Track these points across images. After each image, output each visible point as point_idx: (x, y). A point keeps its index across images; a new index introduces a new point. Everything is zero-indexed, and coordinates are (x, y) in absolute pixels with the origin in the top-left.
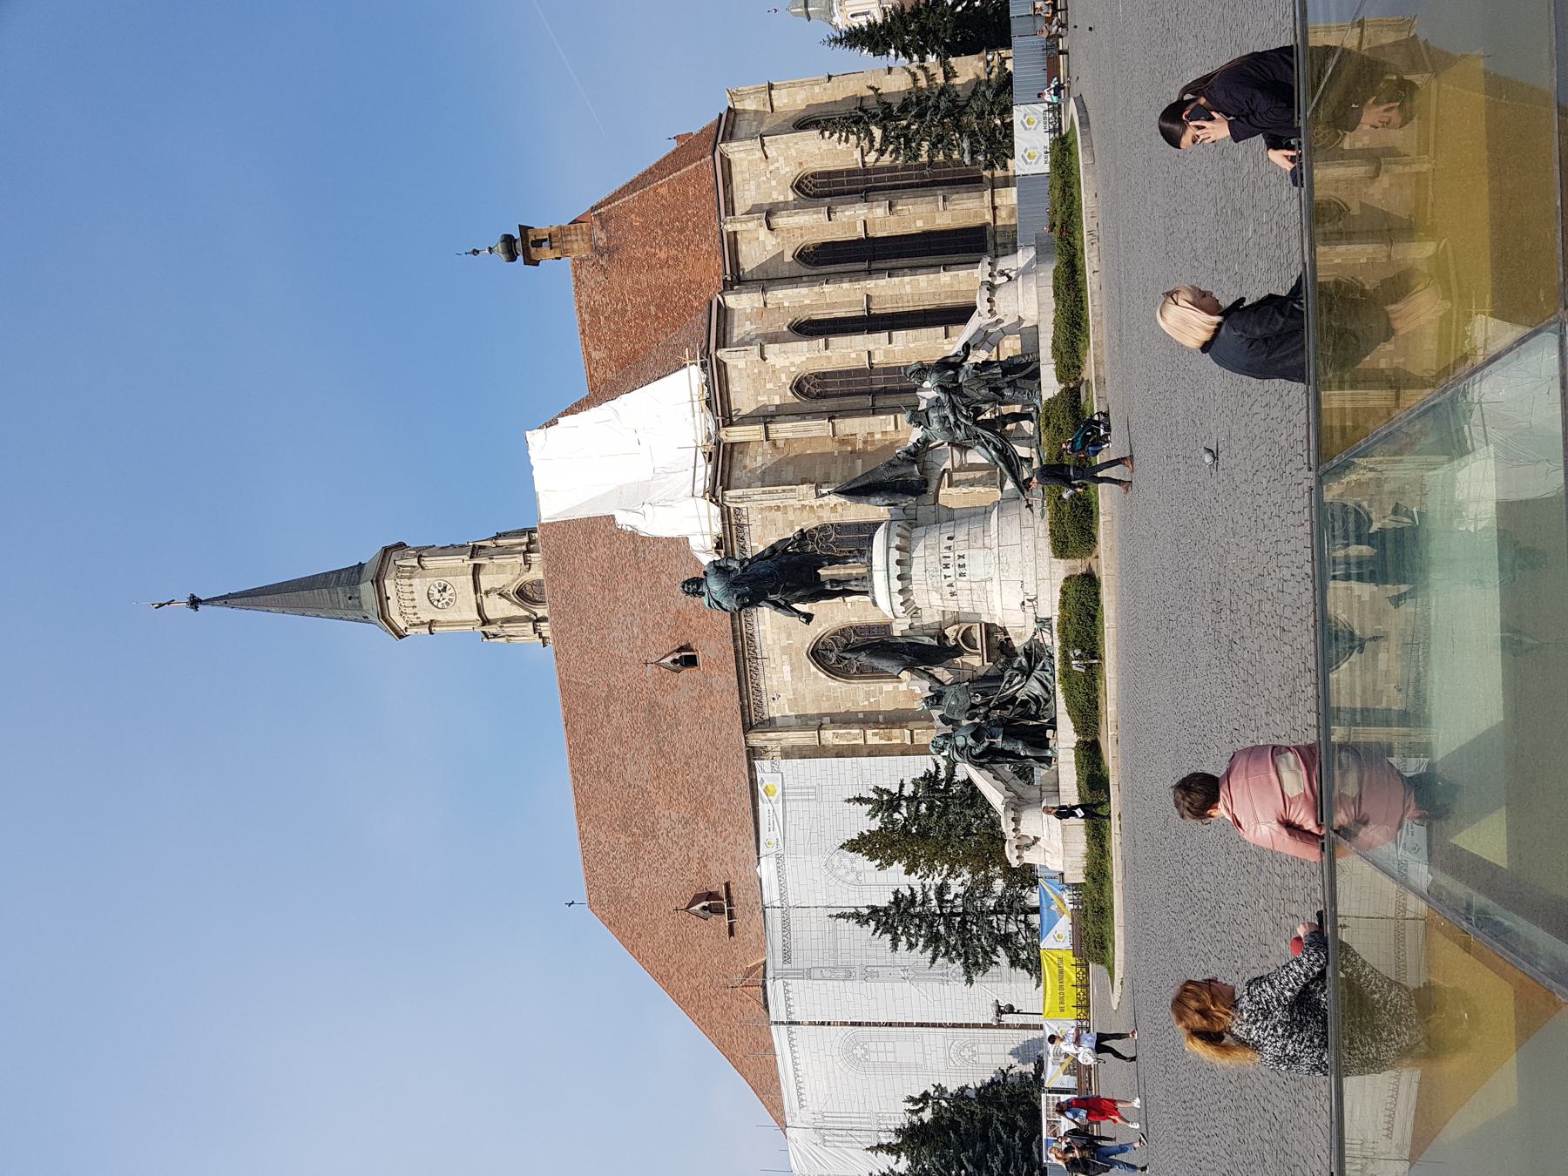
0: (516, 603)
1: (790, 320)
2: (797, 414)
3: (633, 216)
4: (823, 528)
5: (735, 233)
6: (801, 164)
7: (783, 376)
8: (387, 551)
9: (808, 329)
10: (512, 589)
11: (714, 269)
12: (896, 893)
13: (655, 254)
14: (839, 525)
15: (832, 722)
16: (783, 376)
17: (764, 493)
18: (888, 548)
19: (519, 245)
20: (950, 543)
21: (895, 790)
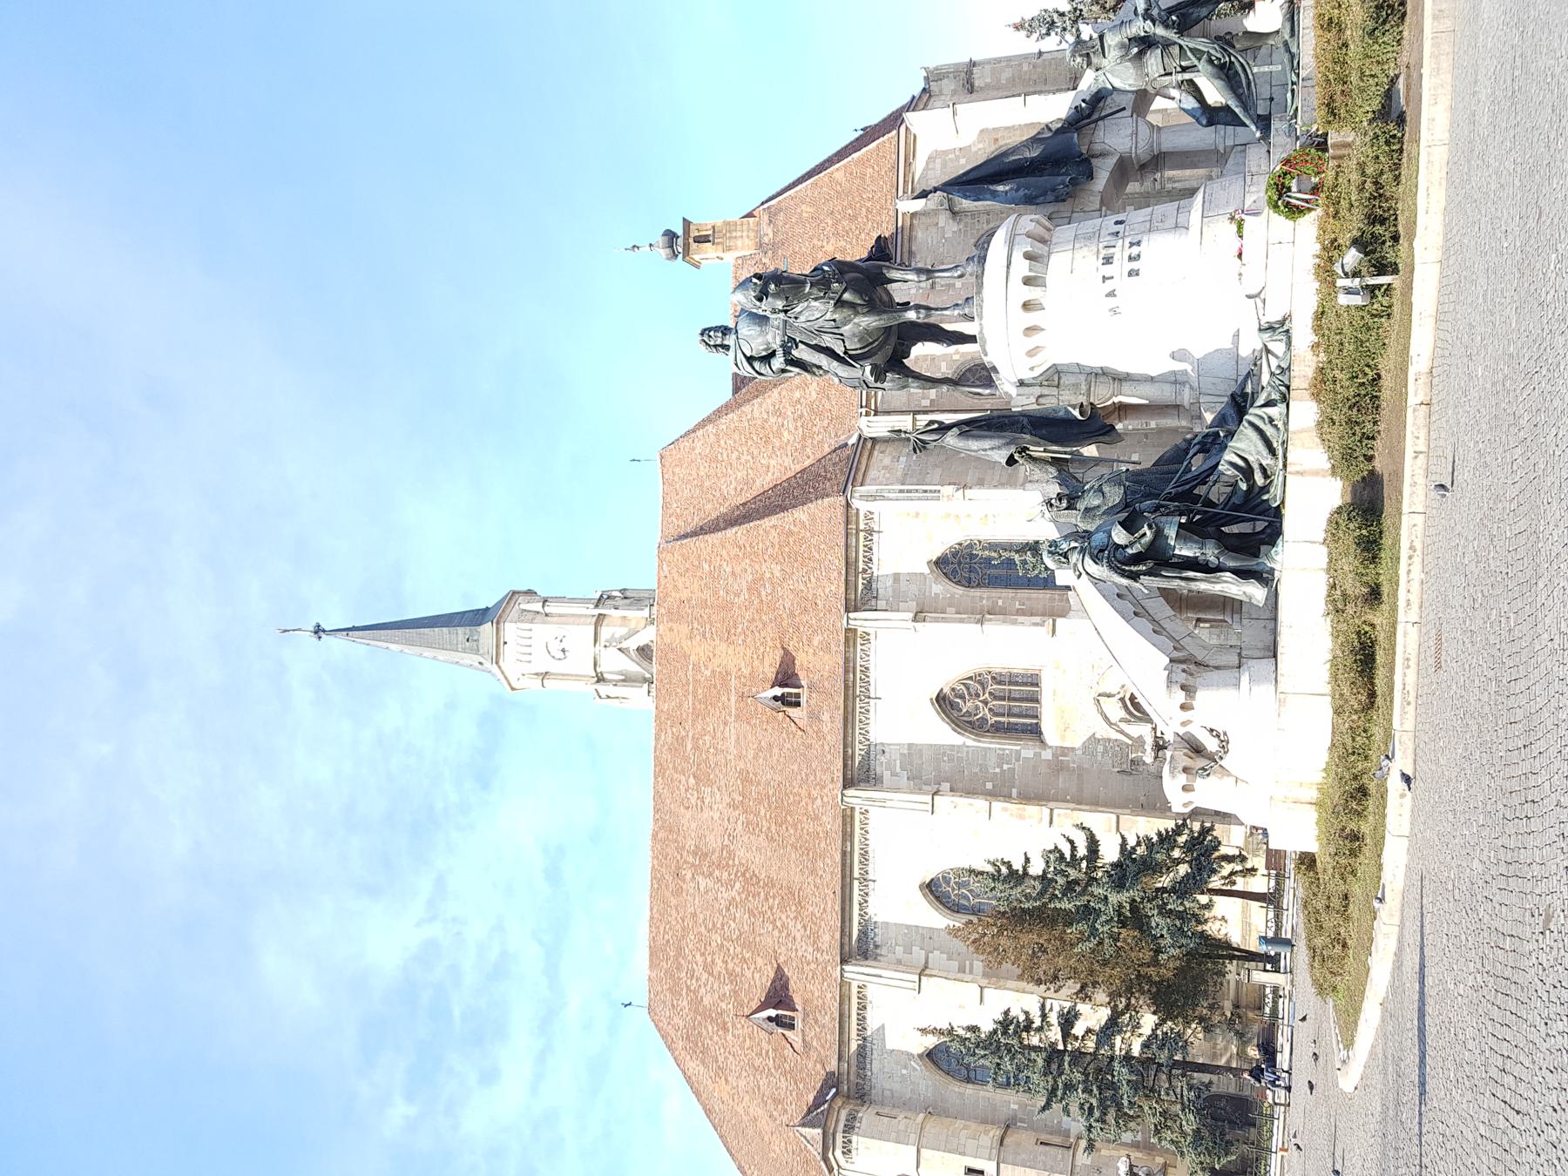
0: (633, 660)
3: (804, 207)
6: (996, 140)
7: (943, 365)
8: (514, 593)
10: (633, 644)
12: (1007, 1013)
16: (943, 365)
17: (901, 491)
19: (680, 241)
21: (1018, 865)
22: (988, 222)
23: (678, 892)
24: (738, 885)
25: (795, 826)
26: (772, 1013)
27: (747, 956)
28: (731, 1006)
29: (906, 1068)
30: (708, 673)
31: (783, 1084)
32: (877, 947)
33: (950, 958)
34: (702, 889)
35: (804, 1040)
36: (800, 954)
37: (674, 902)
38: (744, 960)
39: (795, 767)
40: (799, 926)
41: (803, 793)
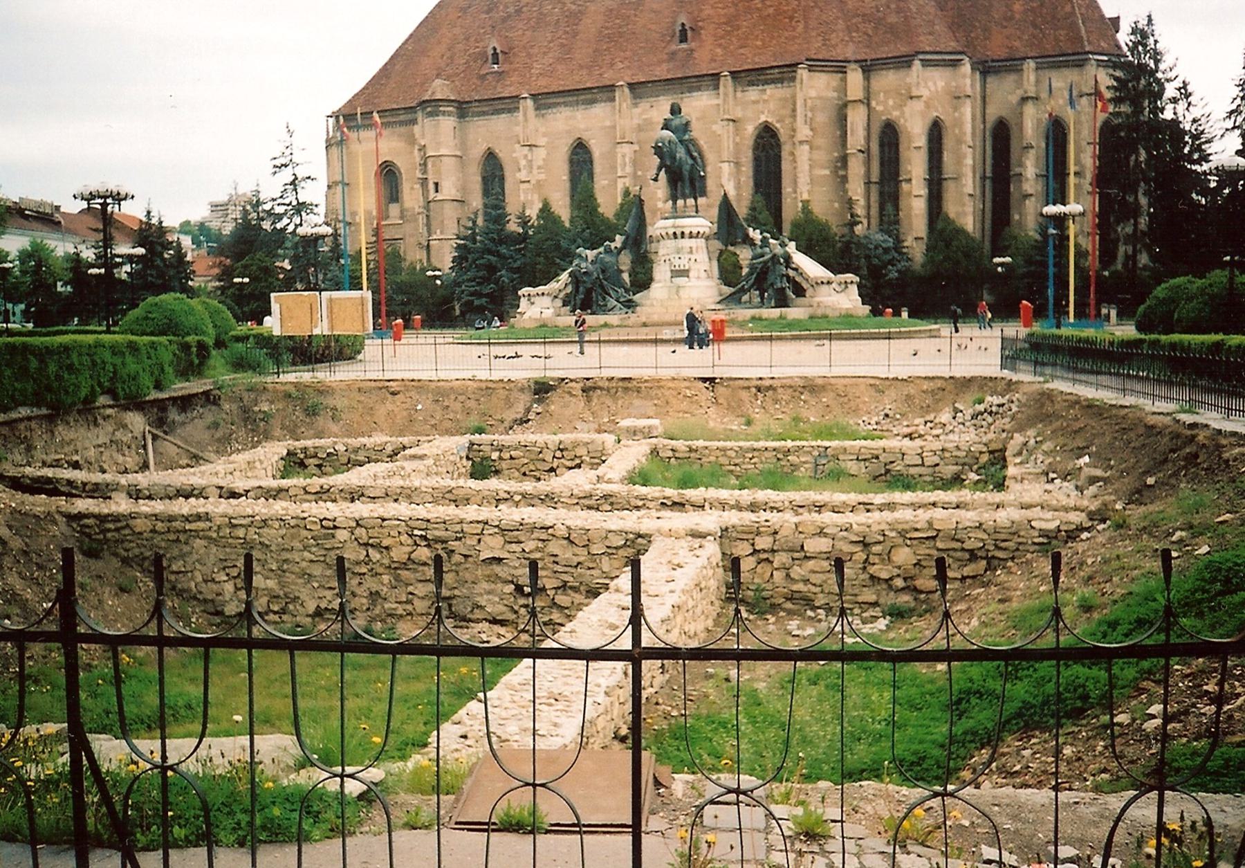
1: (942, 117)
2: (868, 125)
5: (1022, 70)
9: (936, 133)
11: (996, 48)
14: (780, 157)
15: (635, 151)
17: (805, 100)
18: (690, 226)
20: (693, 260)
22: (1016, 124)
24: (574, 7)
26: (498, 51)
32: (543, 115)
33: (544, 160)
38: (530, 19)
40: (551, 61)
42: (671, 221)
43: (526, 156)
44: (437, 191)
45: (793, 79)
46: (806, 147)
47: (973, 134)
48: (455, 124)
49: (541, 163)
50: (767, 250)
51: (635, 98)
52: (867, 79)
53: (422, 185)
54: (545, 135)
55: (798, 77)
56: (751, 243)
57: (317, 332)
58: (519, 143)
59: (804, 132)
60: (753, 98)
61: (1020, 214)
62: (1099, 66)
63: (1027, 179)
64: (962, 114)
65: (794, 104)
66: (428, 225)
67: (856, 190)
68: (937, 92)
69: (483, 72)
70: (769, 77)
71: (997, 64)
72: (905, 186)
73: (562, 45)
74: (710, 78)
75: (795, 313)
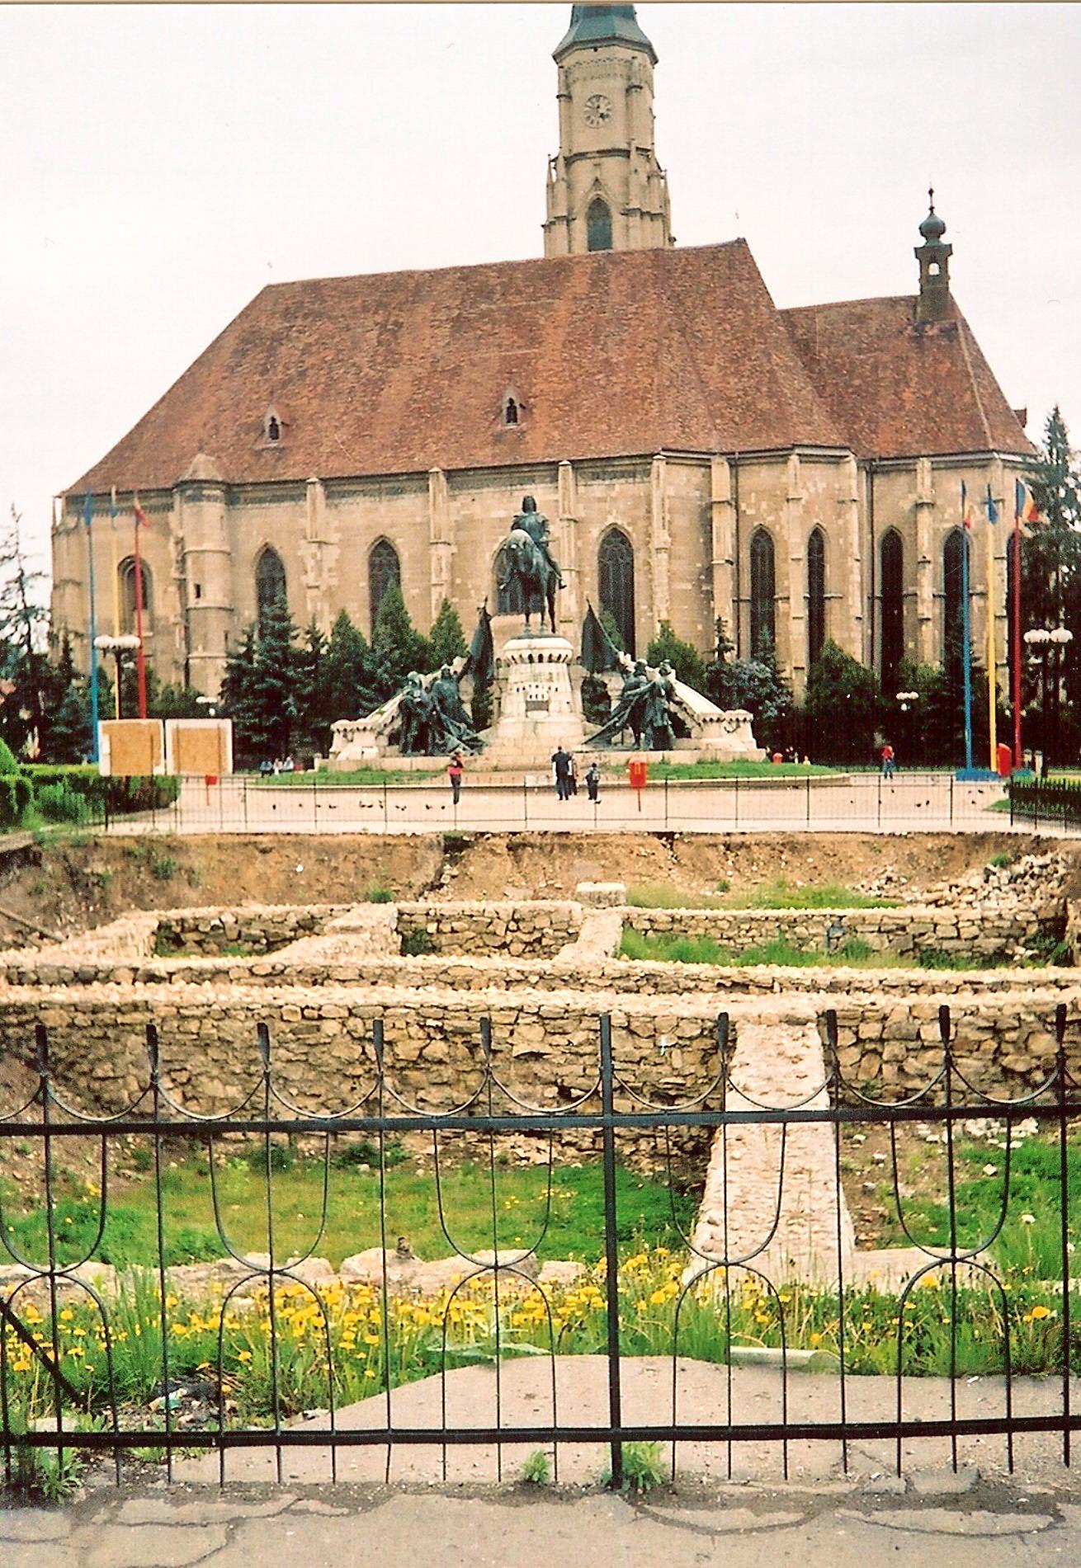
1: (824, 525)
3: (949, 365)
4: (631, 553)
11: (884, 444)
13: (909, 387)
16: (771, 518)
17: (663, 500)
23: (365, 309)
24: (372, 373)
25: (416, 427)
26: (278, 422)
27: (319, 389)
28: (280, 376)
29: (258, 534)
30: (542, 322)
31: (230, 433)
32: (336, 506)
34: (368, 335)
35: (263, 450)
36: (324, 440)
37: (358, 303)
39: (461, 423)
41: (444, 433)
42: (525, 642)
43: (314, 556)
44: (198, 596)
45: (648, 473)
46: (664, 556)
47: (861, 546)
48: (222, 512)
49: (333, 565)
50: (643, 678)
51: (452, 488)
52: (735, 476)
53: (180, 588)
54: (337, 530)
55: (654, 470)
56: (624, 671)
57: (159, 771)
58: (305, 538)
59: (661, 537)
60: (599, 495)
61: (916, 642)
62: (1005, 467)
63: (923, 601)
64: (846, 522)
65: (649, 504)
66: (187, 639)
67: (723, 608)
68: (817, 494)
69: (258, 447)
70: (619, 469)
71: (885, 462)
72: (781, 606)
73: (360, 419)
74: (547, 467)
75: (680, 756)
